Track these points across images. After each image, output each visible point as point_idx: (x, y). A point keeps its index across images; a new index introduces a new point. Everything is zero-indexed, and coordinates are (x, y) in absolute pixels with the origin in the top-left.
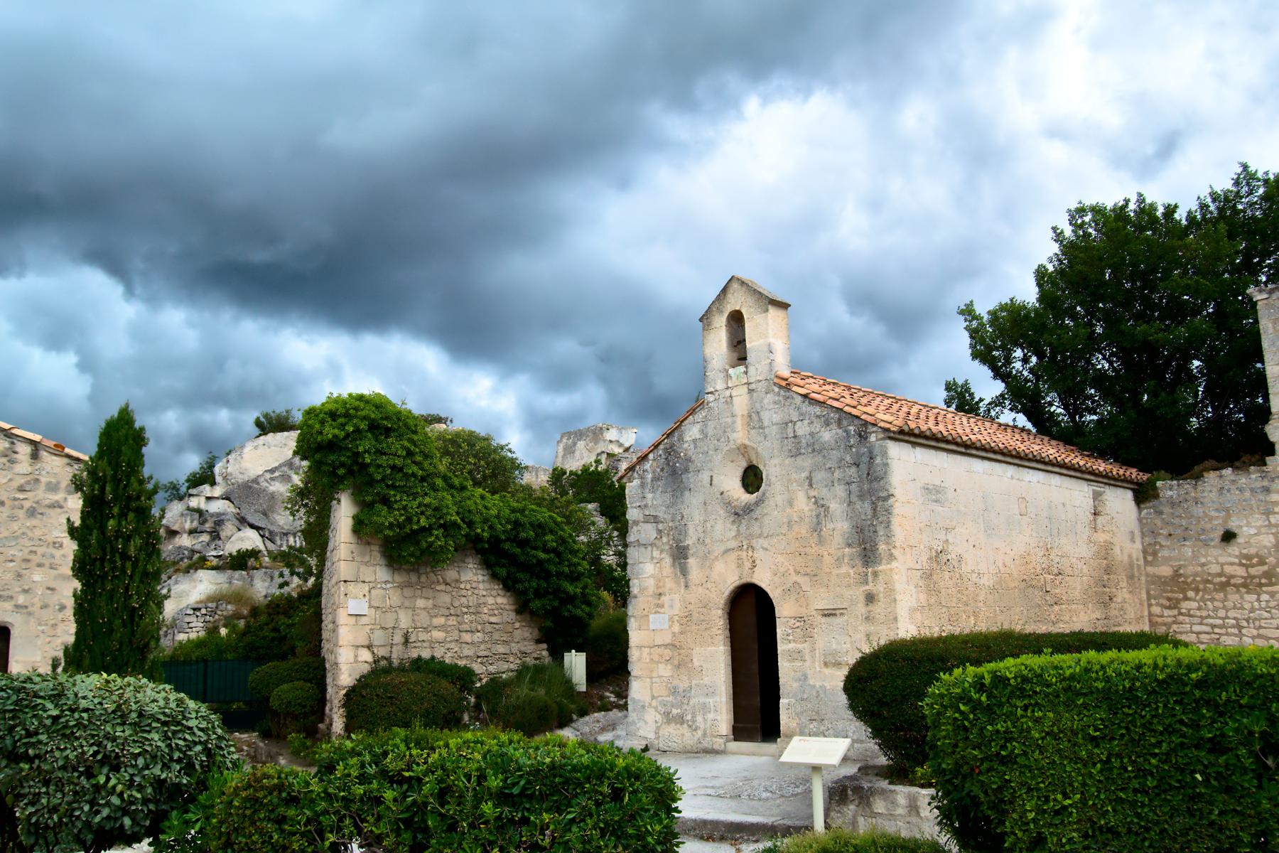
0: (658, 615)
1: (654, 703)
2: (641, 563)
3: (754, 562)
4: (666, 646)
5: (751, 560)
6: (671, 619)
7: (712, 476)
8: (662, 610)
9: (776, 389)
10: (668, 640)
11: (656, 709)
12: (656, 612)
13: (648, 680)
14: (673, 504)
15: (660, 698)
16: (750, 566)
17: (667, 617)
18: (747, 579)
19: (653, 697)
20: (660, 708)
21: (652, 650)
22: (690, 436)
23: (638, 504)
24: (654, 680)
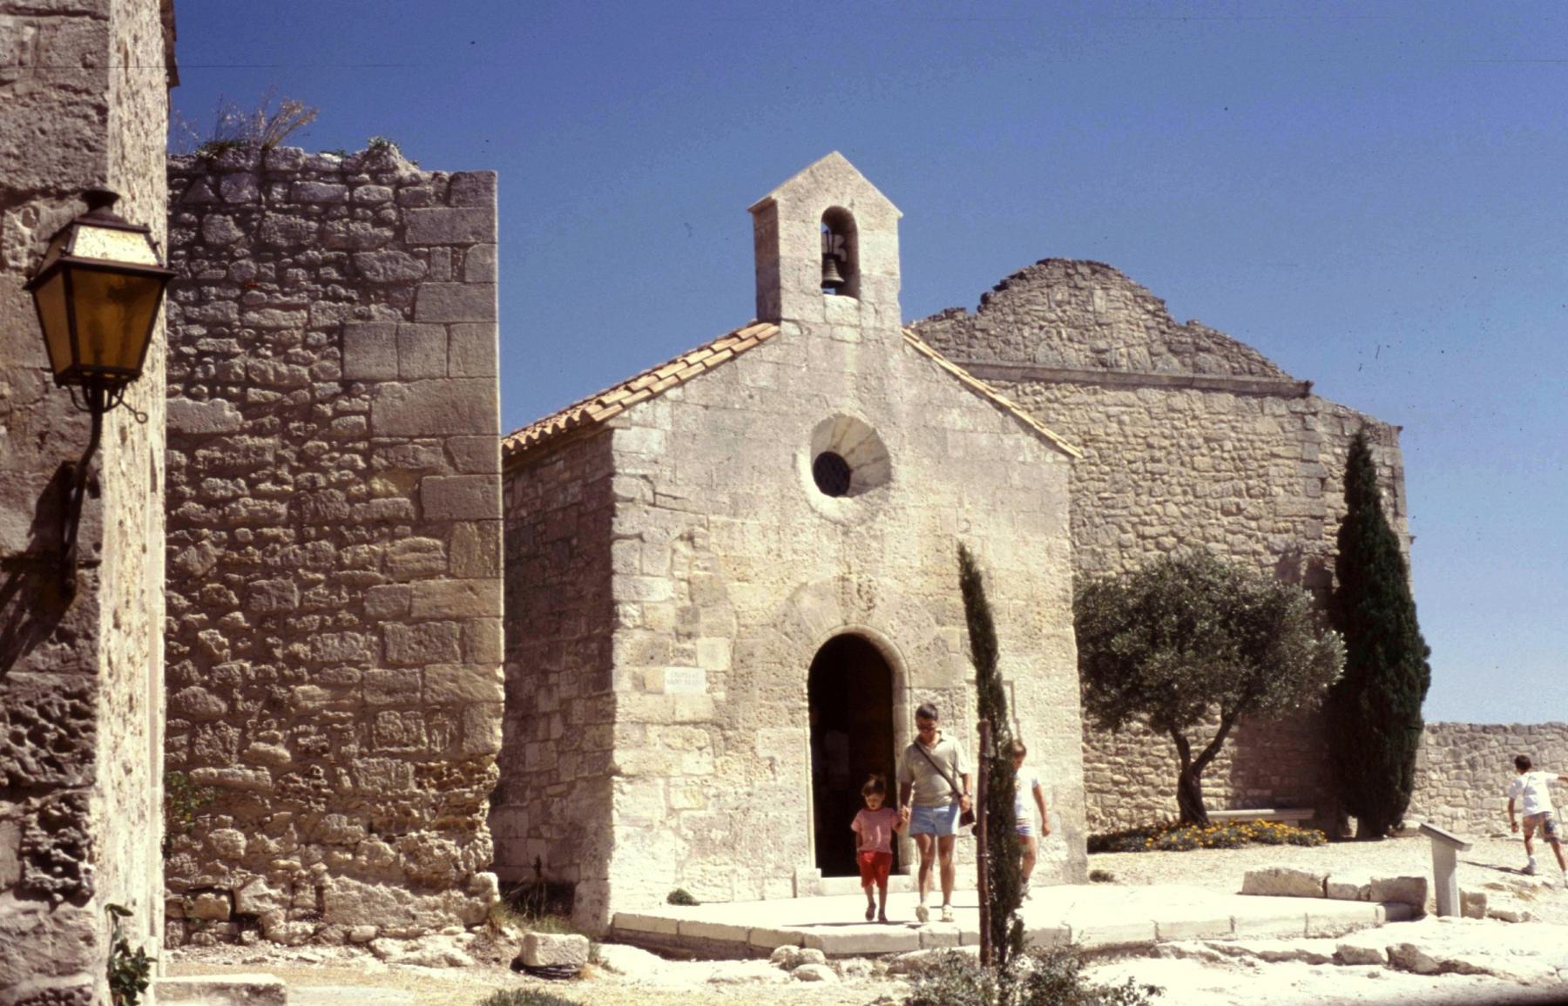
0: (681, 670)
1: (673, 823)
2: (648, 575)
3: (870, 600)
4: (695, 724)
5: (865, 597)
6: (711, 676)
7: (794, 456)
8: (692, 662)
9: (909, 349)
10: (705, 711)
11: (676, 831)
12: (678, 665)
13: (661, 781)
14: (718, 485)
15: (685, 814)
16: (864, 605)
17: (702, 674)
18: (854, 625)
19: (672, 811)
20: (684, 831)
21: (667, 730)
22: (753, 381)
23: (640, 472)
24: (672, 781)
